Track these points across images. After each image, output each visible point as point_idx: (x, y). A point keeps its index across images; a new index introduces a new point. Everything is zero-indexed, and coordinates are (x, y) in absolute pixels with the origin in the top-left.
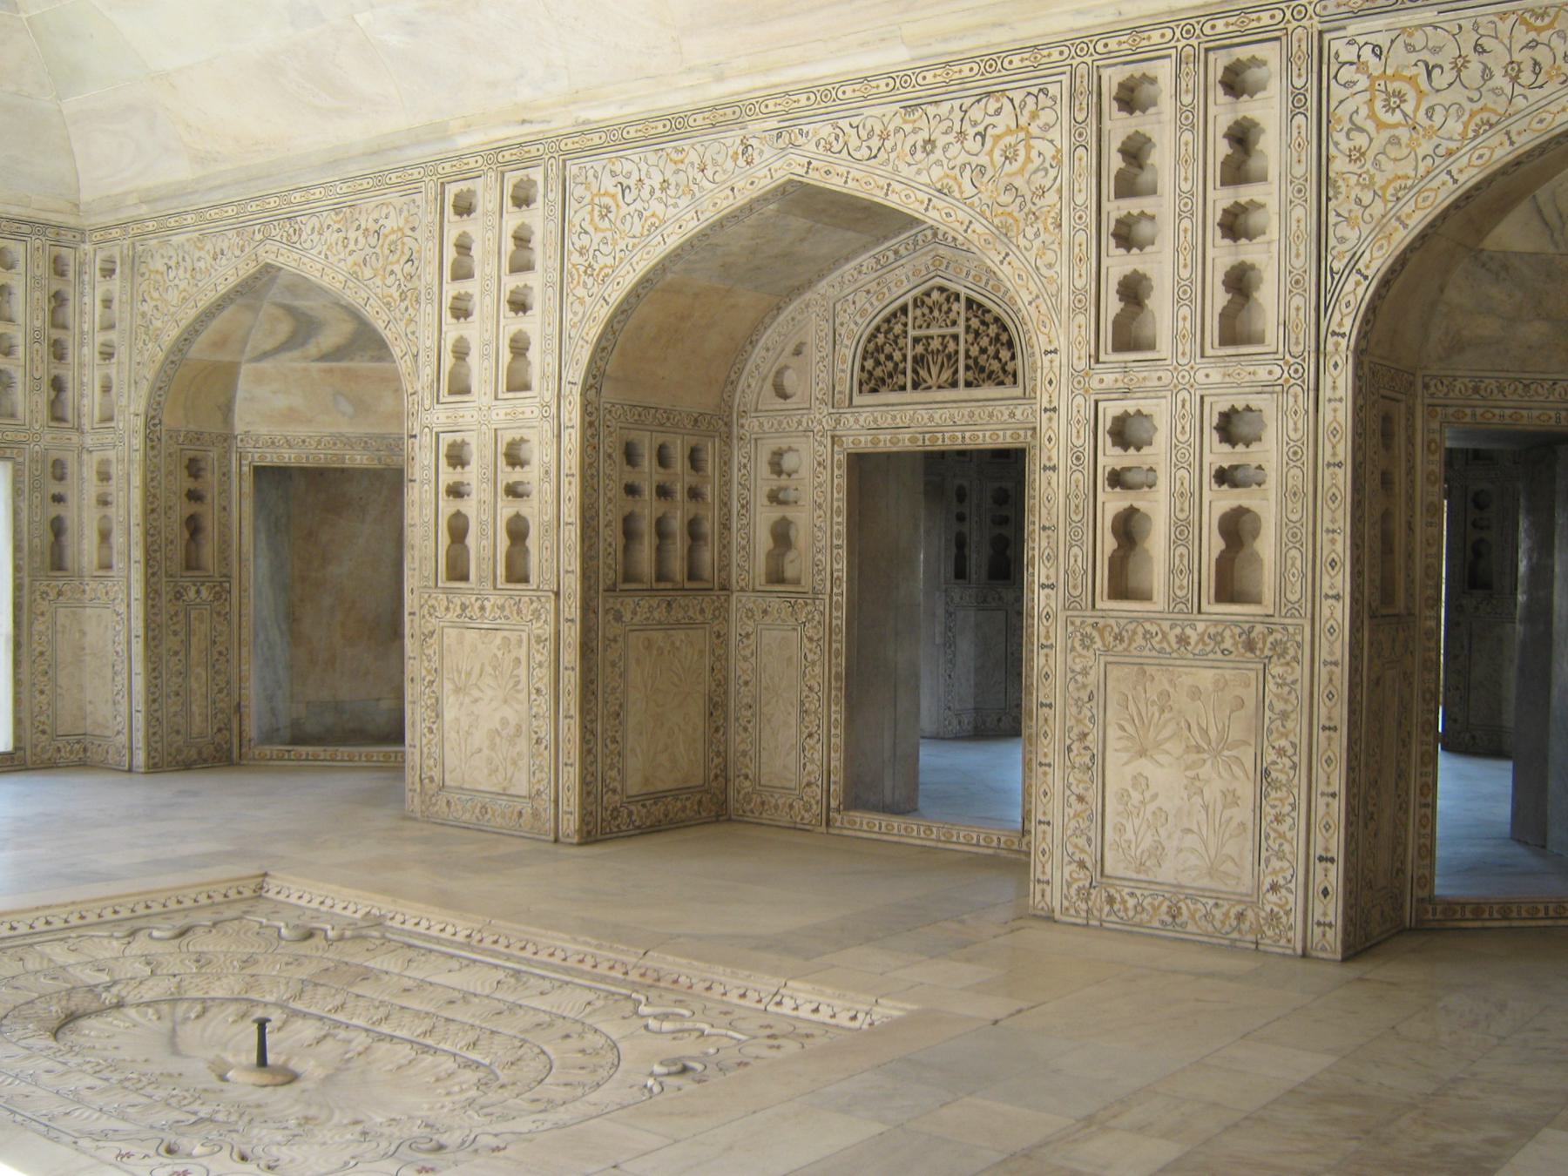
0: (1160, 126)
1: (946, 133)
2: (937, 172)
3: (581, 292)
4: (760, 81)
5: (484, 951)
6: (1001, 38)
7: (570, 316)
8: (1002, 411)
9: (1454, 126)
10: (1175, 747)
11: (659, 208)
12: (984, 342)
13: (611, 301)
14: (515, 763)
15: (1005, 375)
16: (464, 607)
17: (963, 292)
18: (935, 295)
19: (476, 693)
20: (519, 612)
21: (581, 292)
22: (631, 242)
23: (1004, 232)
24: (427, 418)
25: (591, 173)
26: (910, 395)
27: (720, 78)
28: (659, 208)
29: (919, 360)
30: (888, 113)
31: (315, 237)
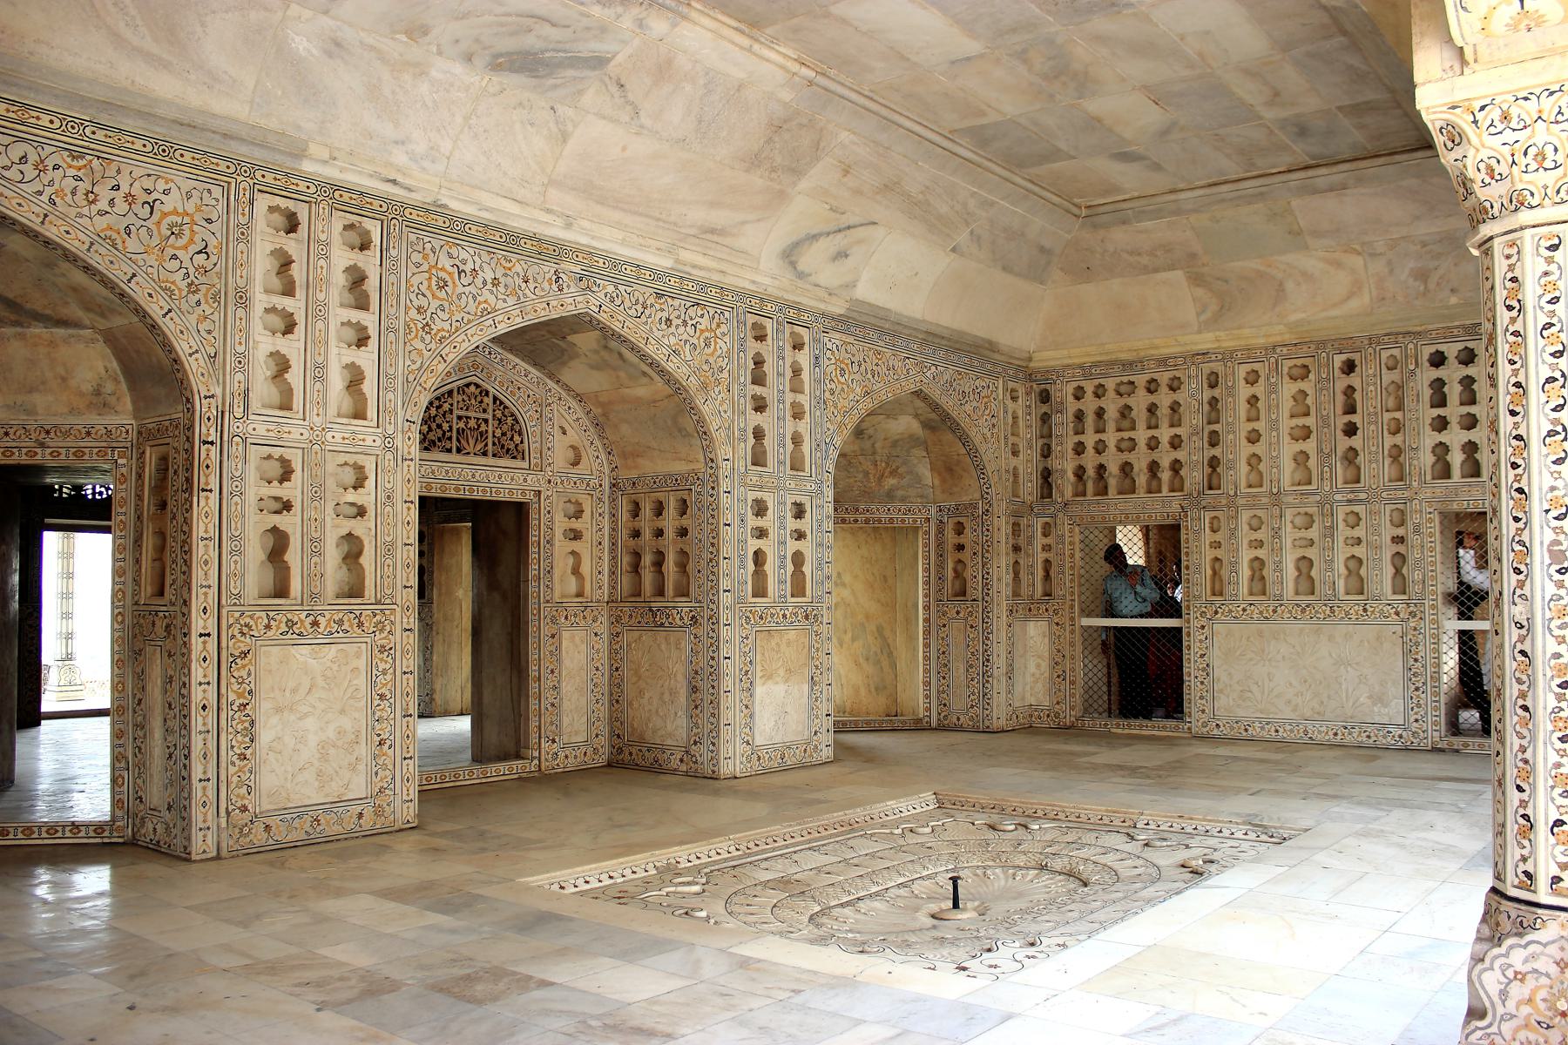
0: (767, 349)
1: (678, 317)
2: (673, 340)
3: (419, 345)
4: (584, 240)
5: (757, 854)
6: (716, 277)
7: (408, 363)
8: (519, 477)
9: (858, 390)
10: (781, 672)
11: (492, 299)
12: (505, 428)
13: (449, 359)
14: (354, 769)
15: (516, 453)
16: (290, 624)
17: (492, 391)
18: (472, 388)
19: (304, 709)
20: (360, 624)
21: (421, 346)
22: (467, 317)
23: (704, 387)
24: (237, 427)
25: (428, 246)
26: (454, 457)
27: (569, 226)
28: (492, 299)
29: (460, 432)
30: (645, 293)
31: (30, 172)
